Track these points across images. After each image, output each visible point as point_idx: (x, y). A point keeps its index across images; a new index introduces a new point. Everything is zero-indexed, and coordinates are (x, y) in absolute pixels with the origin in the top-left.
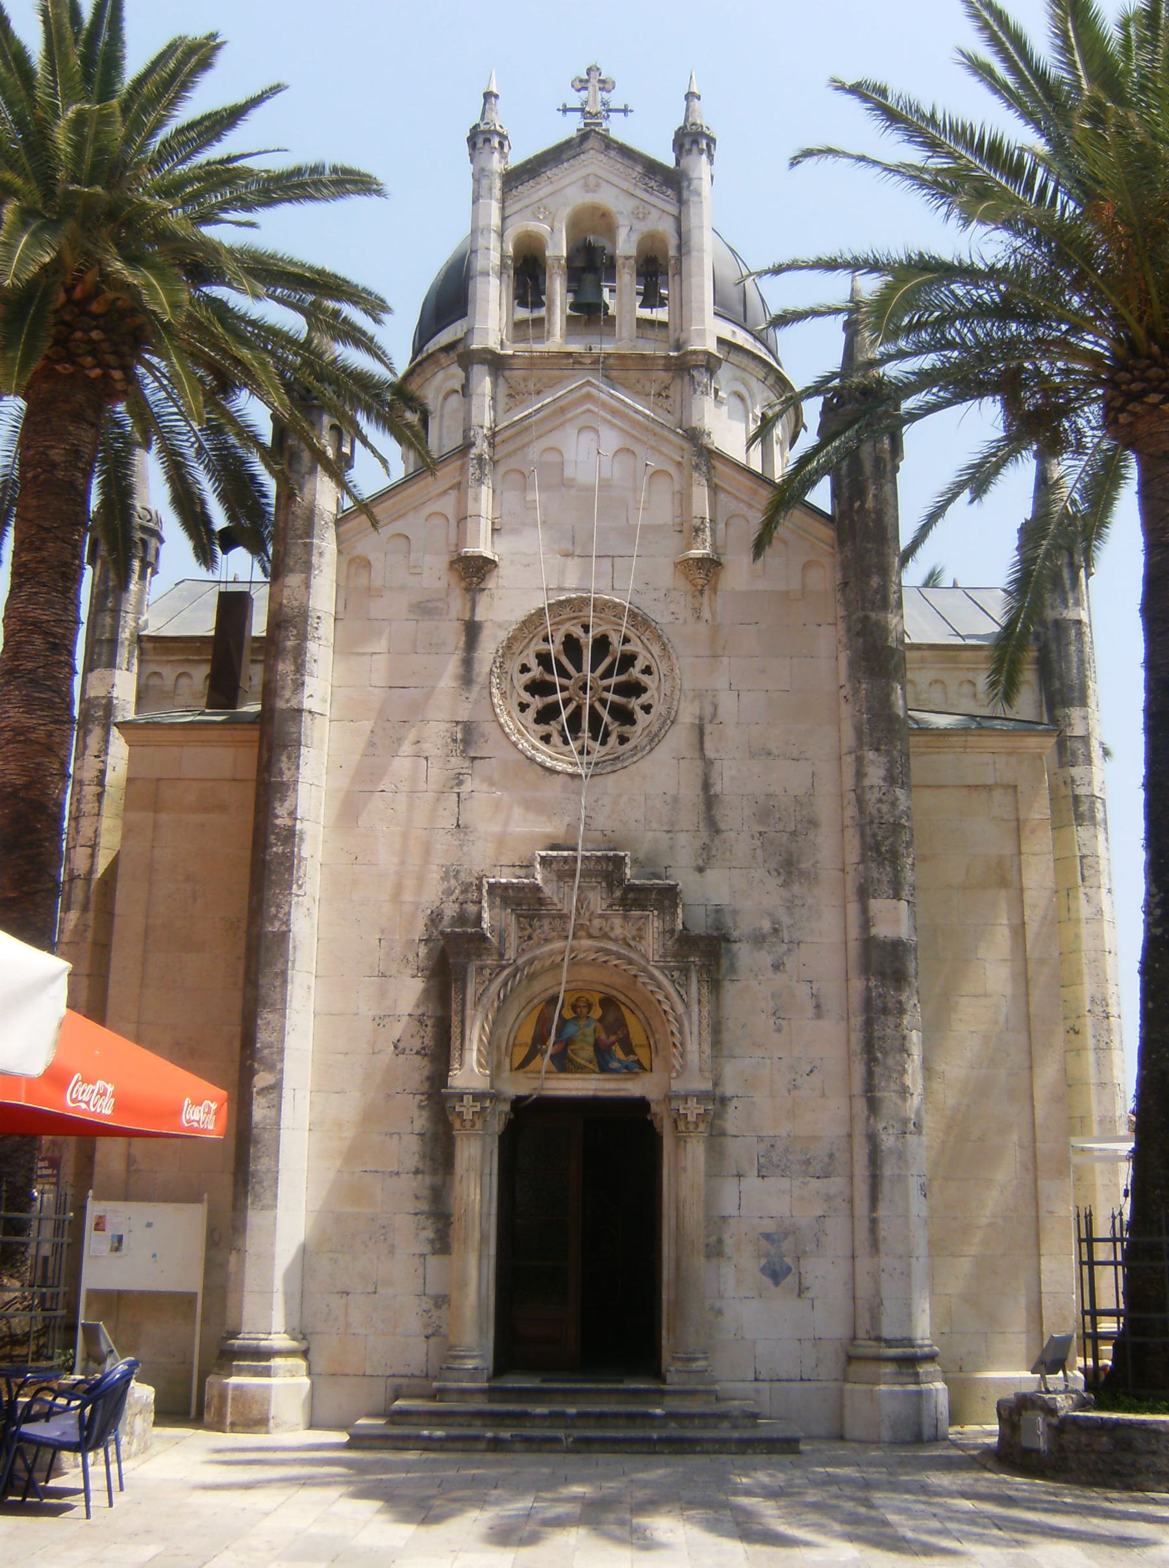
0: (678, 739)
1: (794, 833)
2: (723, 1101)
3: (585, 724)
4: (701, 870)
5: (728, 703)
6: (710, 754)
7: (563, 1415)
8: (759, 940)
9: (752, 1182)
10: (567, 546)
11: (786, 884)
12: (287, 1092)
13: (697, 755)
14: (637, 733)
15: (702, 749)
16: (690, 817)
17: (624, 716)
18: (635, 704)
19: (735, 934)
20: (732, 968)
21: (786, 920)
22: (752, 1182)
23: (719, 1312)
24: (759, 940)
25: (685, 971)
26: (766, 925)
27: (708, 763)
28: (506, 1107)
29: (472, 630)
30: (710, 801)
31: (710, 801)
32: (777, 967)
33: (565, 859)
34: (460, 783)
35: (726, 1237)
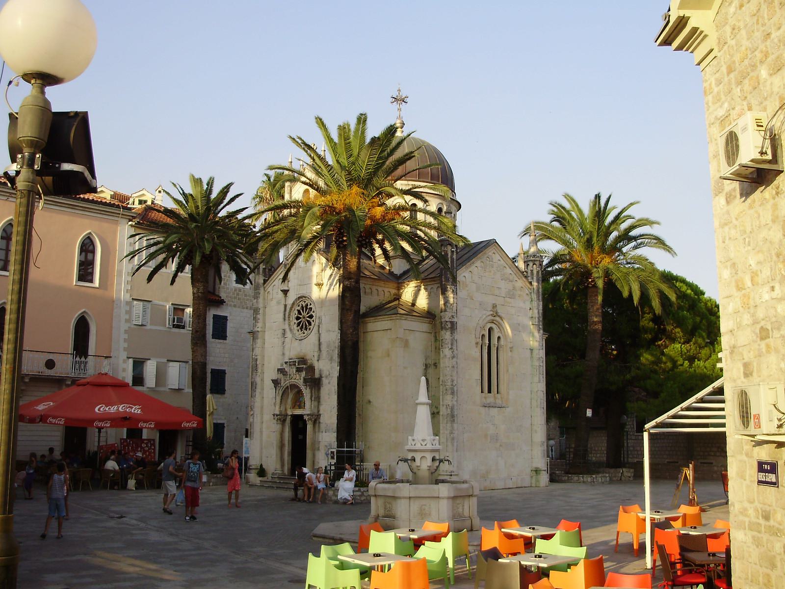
0: (315, 330)
1: (333, 350)
2: (320, 415)
3: (304, 327)
4: (318, 361)
5: (323, 318)
6: (320, 332)
7: (281, 482)
8: (327, 377)
9: (324, 433)
10: (299, 283)
11: (331, 363)
12: (255, 416)
13: (318, 332)
14: (311, 327)
15: (319, 331)
16: (317, 349)
17: (310, 324)
18: (311, 320)
19: (323, 376)
20: (322, 384)
21: (331, 372)
22: (324, 433)
23: (318, 463)
24: (327, 377)
25: (306, 385)
26: (328, 373)
27: (320, 334)
28: (290, 417)
29: (285, 306)
30: (320, 344)
31: (320, 344)
32: (329, 383)
33: (293, 362)
34: (283, 344)
35: (320, 445)
